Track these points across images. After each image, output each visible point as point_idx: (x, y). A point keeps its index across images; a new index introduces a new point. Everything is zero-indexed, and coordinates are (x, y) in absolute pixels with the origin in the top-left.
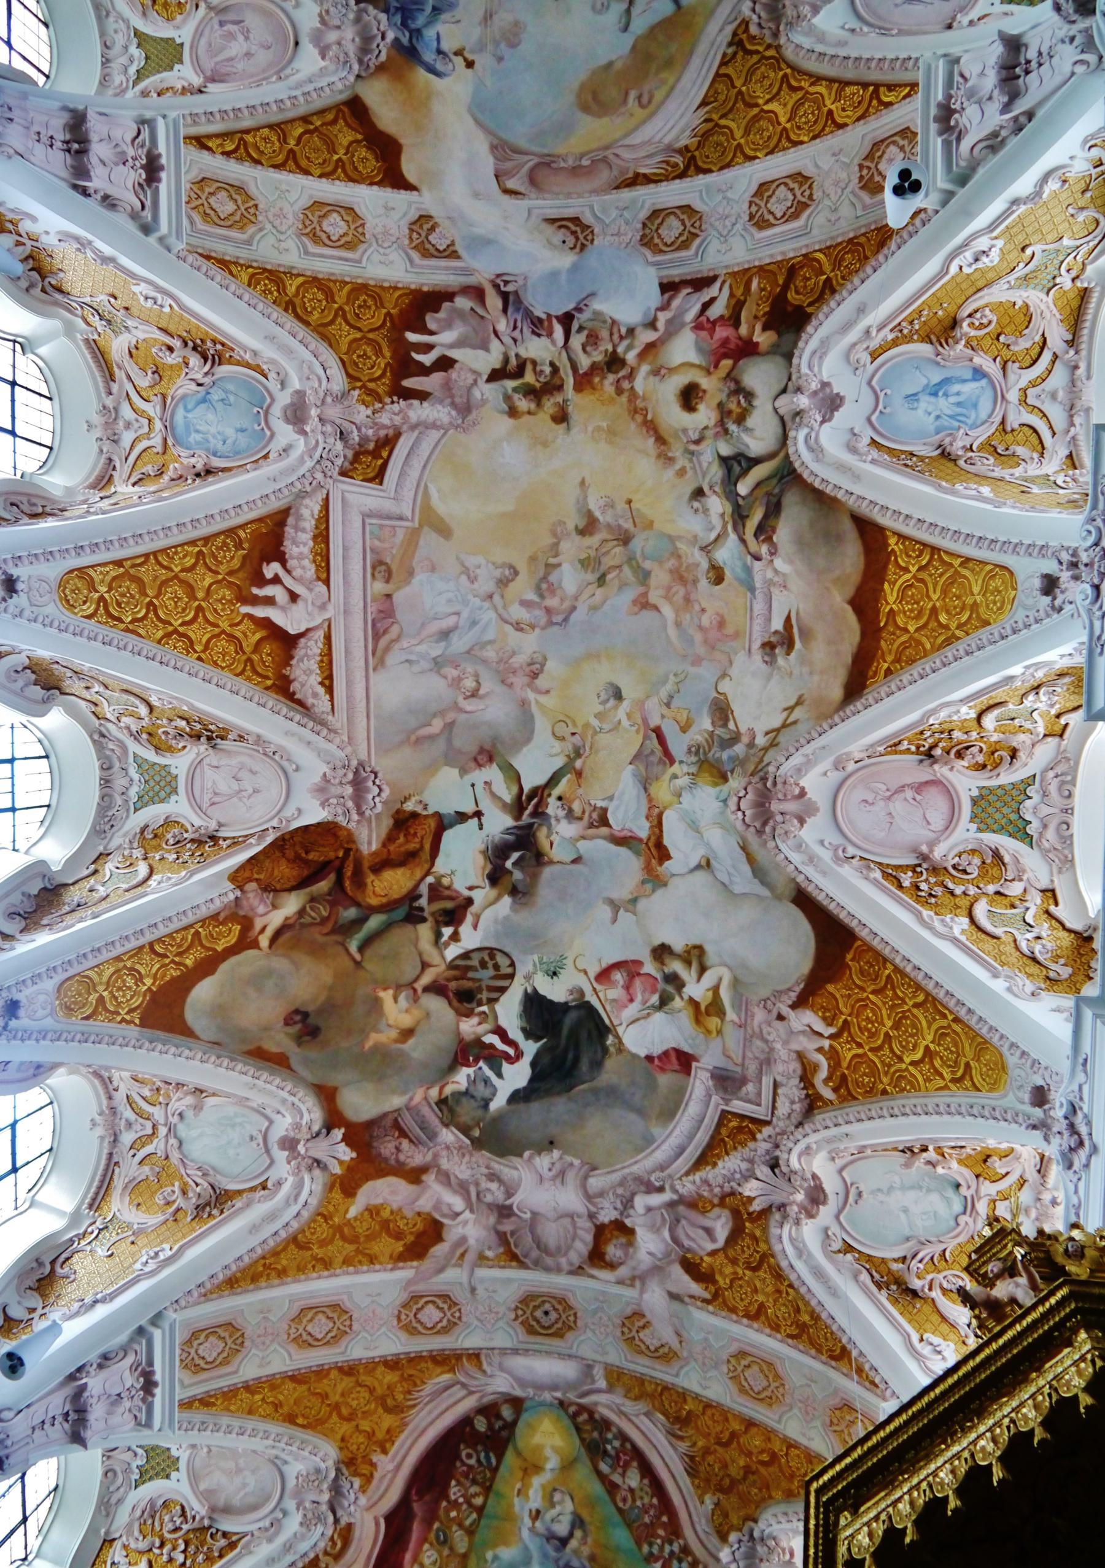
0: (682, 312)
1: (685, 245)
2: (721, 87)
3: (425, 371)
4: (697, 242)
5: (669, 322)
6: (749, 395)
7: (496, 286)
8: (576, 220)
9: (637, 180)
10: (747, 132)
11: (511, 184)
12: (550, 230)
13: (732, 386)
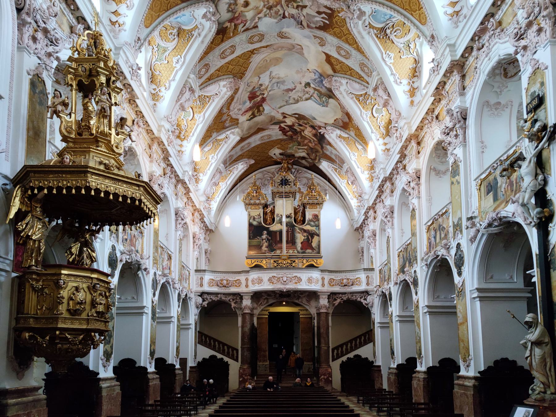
0: (251, 23)
1: (252, 36)
2: (247, 66)
3: (324, 13)
4: (249, 37)
5: (255, 20)
6: (228, 11)
7: (304, 27)
8: (282, 38)
9: (267, 47)
10: (239, 61)
11: (299, 47)
12: (289, 37)
13: (234, 11)
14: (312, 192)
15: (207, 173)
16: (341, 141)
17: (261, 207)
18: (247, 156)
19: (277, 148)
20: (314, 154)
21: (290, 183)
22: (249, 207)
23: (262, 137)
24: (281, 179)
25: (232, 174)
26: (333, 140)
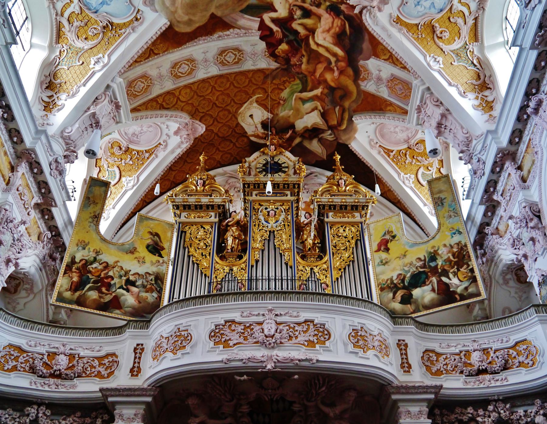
14: (338, 185)
15: (77, 92)
16: (400, 30)
17: (213, 214)
18: (187, 103)
19: (257, 101)
20: (337, 109)
21: (286, 170)
22: (183, 214)
23: (223, 52)
24: (264, 162)
25: (153, 159)
26: (384, 28)
